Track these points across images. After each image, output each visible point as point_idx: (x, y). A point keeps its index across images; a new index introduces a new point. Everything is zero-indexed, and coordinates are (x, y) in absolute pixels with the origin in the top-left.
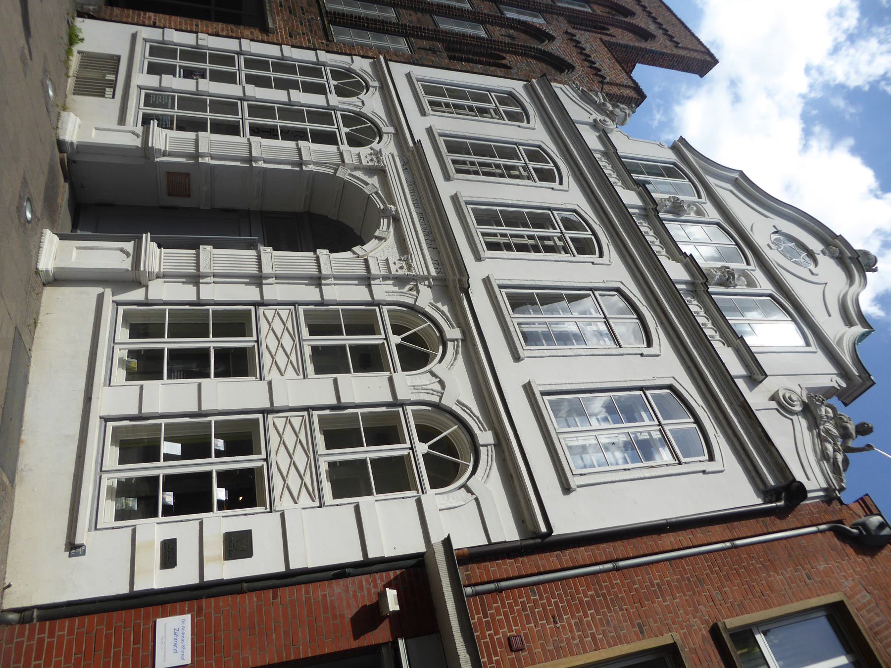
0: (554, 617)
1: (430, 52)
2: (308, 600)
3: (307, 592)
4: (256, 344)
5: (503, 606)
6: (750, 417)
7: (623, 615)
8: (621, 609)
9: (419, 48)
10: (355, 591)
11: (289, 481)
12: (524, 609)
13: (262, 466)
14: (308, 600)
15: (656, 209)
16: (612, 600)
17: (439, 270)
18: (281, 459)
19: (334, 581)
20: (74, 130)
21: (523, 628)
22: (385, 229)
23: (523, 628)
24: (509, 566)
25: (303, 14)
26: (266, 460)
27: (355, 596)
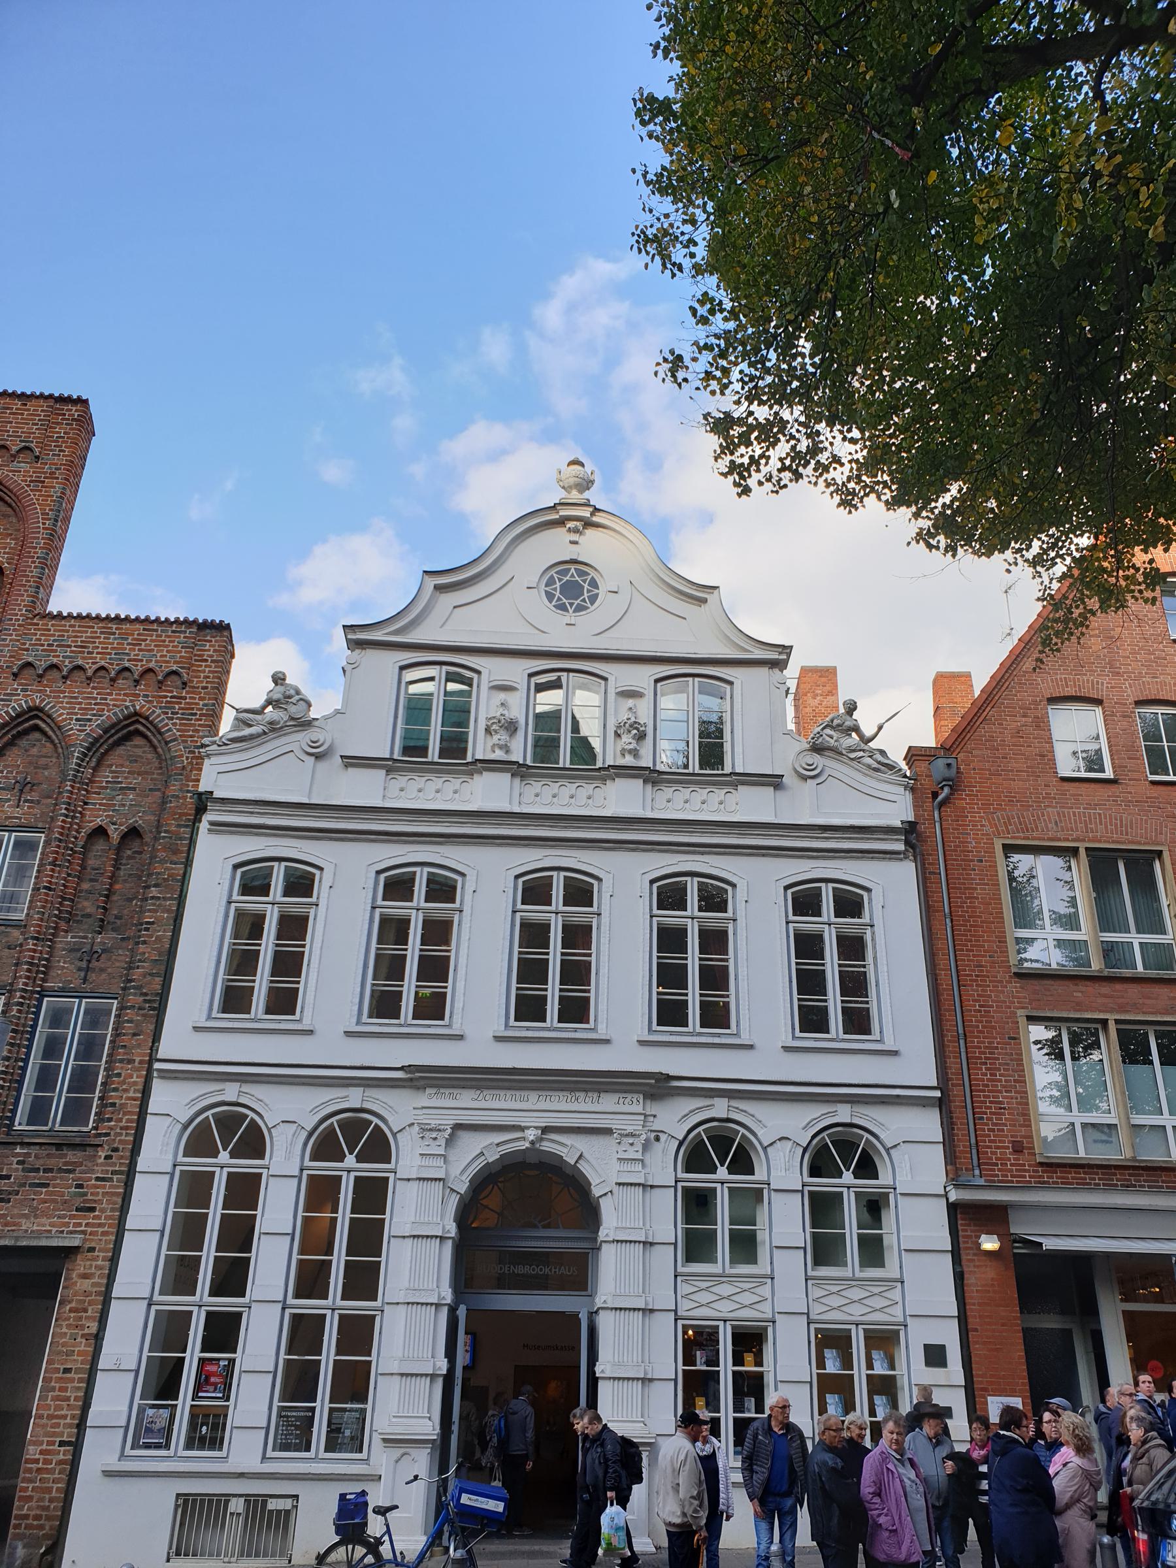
0: (1001, 1108)
1: (94, 964)
2: (980, 1304)
3: (974, 1304)
4: (728, 1323)
5: (990, 1147)
6: (836, 831)
7: (1002, 1049)
8: (997, 1048)
9: (85, 980)
10: (975, 1266)
11: (835, 1305)
12: (993, 1130)
13: (864, 1329)
14: (980, 1304)
16: (990, 1053)
17: (635, 1100)
18: (856, 1311)
19: (965, 1282)
20: (403, 1541)
21: (1007, 1136)
22: (565, 1150)
23: (1007, 1136)
24: (959, 1133)
25: (8, 1177)
26: (857, 1325)
27: (978, 1267)
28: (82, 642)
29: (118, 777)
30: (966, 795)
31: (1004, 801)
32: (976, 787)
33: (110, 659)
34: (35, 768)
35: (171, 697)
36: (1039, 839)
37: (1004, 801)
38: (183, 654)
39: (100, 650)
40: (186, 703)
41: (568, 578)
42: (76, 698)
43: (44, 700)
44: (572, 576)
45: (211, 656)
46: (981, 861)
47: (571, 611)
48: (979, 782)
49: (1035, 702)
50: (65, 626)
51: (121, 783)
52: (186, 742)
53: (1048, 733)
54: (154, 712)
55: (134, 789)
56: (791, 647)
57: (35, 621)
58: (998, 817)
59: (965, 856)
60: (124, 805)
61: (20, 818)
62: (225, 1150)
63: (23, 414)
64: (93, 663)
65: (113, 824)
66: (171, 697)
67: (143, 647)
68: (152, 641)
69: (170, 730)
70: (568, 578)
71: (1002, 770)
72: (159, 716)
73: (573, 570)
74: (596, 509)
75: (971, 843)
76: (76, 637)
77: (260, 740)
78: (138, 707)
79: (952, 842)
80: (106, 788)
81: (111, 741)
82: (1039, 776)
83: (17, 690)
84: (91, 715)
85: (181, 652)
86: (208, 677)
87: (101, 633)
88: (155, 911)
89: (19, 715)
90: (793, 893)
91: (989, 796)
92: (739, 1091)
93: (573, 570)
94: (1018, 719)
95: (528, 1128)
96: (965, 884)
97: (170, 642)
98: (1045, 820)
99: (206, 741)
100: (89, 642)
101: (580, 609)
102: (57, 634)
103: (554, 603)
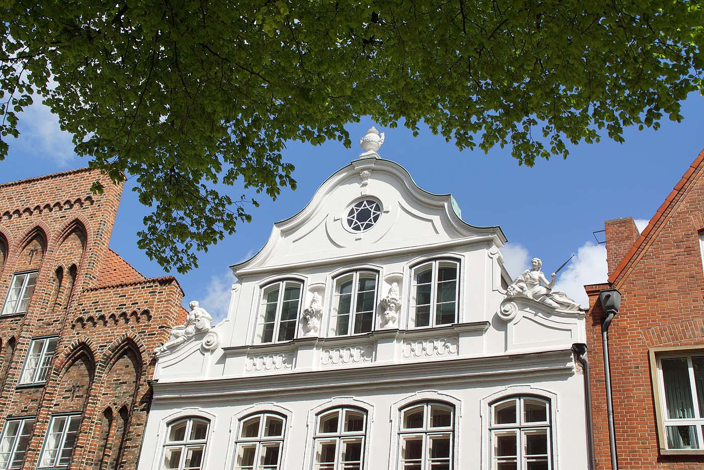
28: (105, 301)
29: (119, 377)
30: (628, 317)
31: (658, 317)
32: (635, 309)
33: (117, 309)
34: (82, 377)
35: (144, 326)
36: (686, 345)
37: (658, 317)
38: (151, 299)
39: (112, 305)
40: (152, 328)
41: (362, 208)
42: (100, 334)
43: (86, 337)
44: (365, 206)
45: (165, 298)
46: (638, 367)
47: (362, 229)
48: (638, 306)
49: (687, 236)
50: (97, 294)
51: (120, 380)
52: (149, 351)
53: (698, 258)
54: (136, 336)
55: (125, 383)
57: (85, 294)
58: (653, 331)
59: (626, 364)
60: (120, 393)
61: (73, 407)
63: (88, 179)
64: (109, 313)
65: (115, 404)
66: (144, 326)
67: (132, 299)
68: (137, 294)
69: (142, 345)
70: (362, 208)
71: (657, 293)
72: (138, 338)
73: (365, 202)
75: (630, 354)
76: (102, 299)
77: (183, 345)
78: (128, 335)
79: (615, 355)
80: (113, 384)
81: (116, 356)
82: (689, 294)
83: (74, 334)
84: (106, 343)
85: (150, 298)
86: (162, 311)
87: (114, 294)
89: (75, 349)
90: (495, 407)
91: (646, 315)
93: (365, 202)
94: (673, 251)
96: (623, 387)
97: (145, 293)
98: (692, 329)
99: (156, 350)
100: (107, 301)
101: (368, 226)
102: (94, 299)
103: (352, 226)
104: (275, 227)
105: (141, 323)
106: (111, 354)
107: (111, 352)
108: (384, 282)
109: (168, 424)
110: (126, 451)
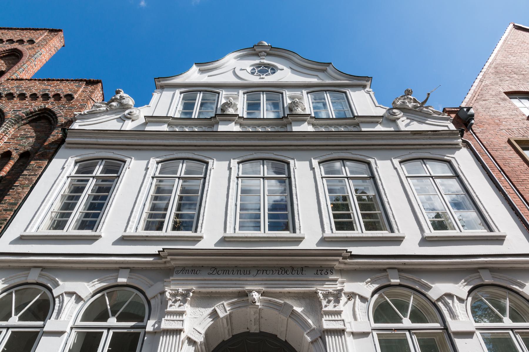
15: (239, 117)
17: (329, 272)
29: (27, 133)
38: (76, 89)
56: (372, 77)
62: (16, 314)
74: (272, 48)
88: (22, 180)
92: (405, 264)
95: (251, 291)
104: (194, 65)
105: (62, 101)
106: (24, 116)
107: (24, 115)
108: (288, 98)
109: (76, 163)
110: (22, 178)
